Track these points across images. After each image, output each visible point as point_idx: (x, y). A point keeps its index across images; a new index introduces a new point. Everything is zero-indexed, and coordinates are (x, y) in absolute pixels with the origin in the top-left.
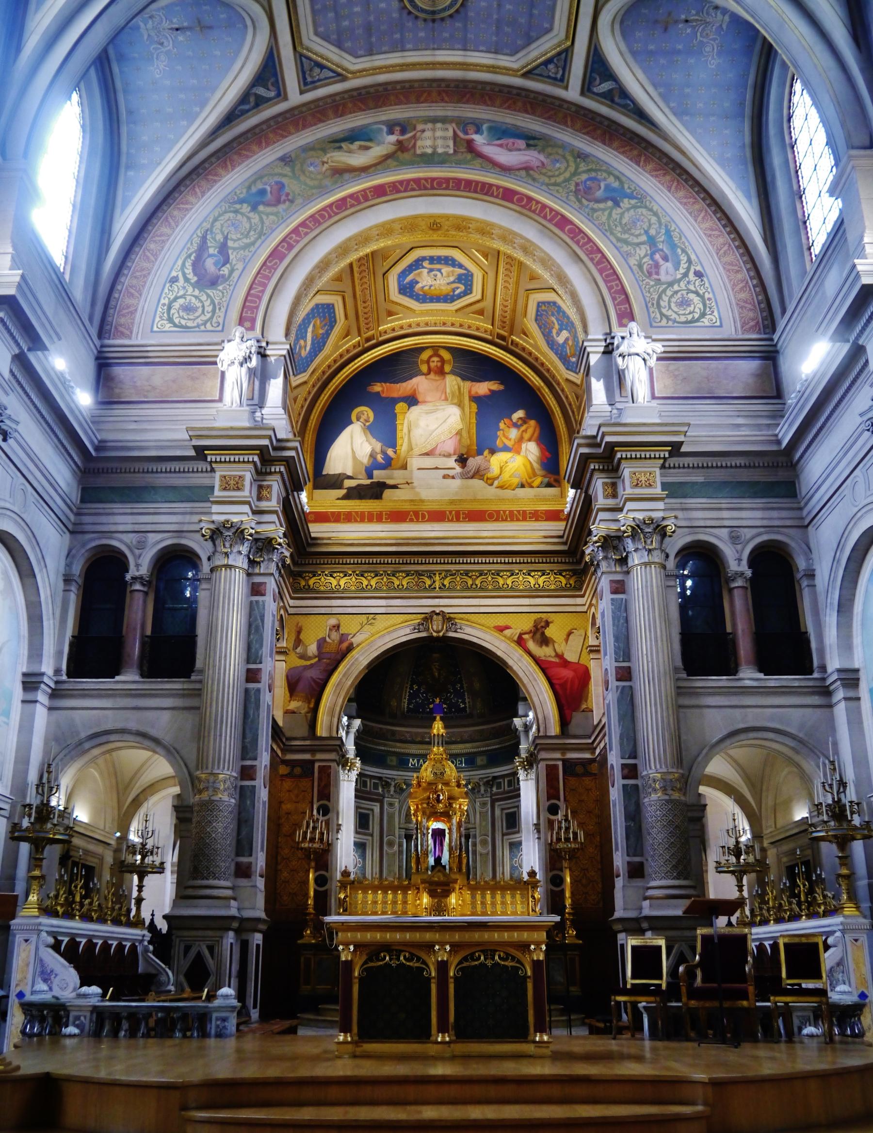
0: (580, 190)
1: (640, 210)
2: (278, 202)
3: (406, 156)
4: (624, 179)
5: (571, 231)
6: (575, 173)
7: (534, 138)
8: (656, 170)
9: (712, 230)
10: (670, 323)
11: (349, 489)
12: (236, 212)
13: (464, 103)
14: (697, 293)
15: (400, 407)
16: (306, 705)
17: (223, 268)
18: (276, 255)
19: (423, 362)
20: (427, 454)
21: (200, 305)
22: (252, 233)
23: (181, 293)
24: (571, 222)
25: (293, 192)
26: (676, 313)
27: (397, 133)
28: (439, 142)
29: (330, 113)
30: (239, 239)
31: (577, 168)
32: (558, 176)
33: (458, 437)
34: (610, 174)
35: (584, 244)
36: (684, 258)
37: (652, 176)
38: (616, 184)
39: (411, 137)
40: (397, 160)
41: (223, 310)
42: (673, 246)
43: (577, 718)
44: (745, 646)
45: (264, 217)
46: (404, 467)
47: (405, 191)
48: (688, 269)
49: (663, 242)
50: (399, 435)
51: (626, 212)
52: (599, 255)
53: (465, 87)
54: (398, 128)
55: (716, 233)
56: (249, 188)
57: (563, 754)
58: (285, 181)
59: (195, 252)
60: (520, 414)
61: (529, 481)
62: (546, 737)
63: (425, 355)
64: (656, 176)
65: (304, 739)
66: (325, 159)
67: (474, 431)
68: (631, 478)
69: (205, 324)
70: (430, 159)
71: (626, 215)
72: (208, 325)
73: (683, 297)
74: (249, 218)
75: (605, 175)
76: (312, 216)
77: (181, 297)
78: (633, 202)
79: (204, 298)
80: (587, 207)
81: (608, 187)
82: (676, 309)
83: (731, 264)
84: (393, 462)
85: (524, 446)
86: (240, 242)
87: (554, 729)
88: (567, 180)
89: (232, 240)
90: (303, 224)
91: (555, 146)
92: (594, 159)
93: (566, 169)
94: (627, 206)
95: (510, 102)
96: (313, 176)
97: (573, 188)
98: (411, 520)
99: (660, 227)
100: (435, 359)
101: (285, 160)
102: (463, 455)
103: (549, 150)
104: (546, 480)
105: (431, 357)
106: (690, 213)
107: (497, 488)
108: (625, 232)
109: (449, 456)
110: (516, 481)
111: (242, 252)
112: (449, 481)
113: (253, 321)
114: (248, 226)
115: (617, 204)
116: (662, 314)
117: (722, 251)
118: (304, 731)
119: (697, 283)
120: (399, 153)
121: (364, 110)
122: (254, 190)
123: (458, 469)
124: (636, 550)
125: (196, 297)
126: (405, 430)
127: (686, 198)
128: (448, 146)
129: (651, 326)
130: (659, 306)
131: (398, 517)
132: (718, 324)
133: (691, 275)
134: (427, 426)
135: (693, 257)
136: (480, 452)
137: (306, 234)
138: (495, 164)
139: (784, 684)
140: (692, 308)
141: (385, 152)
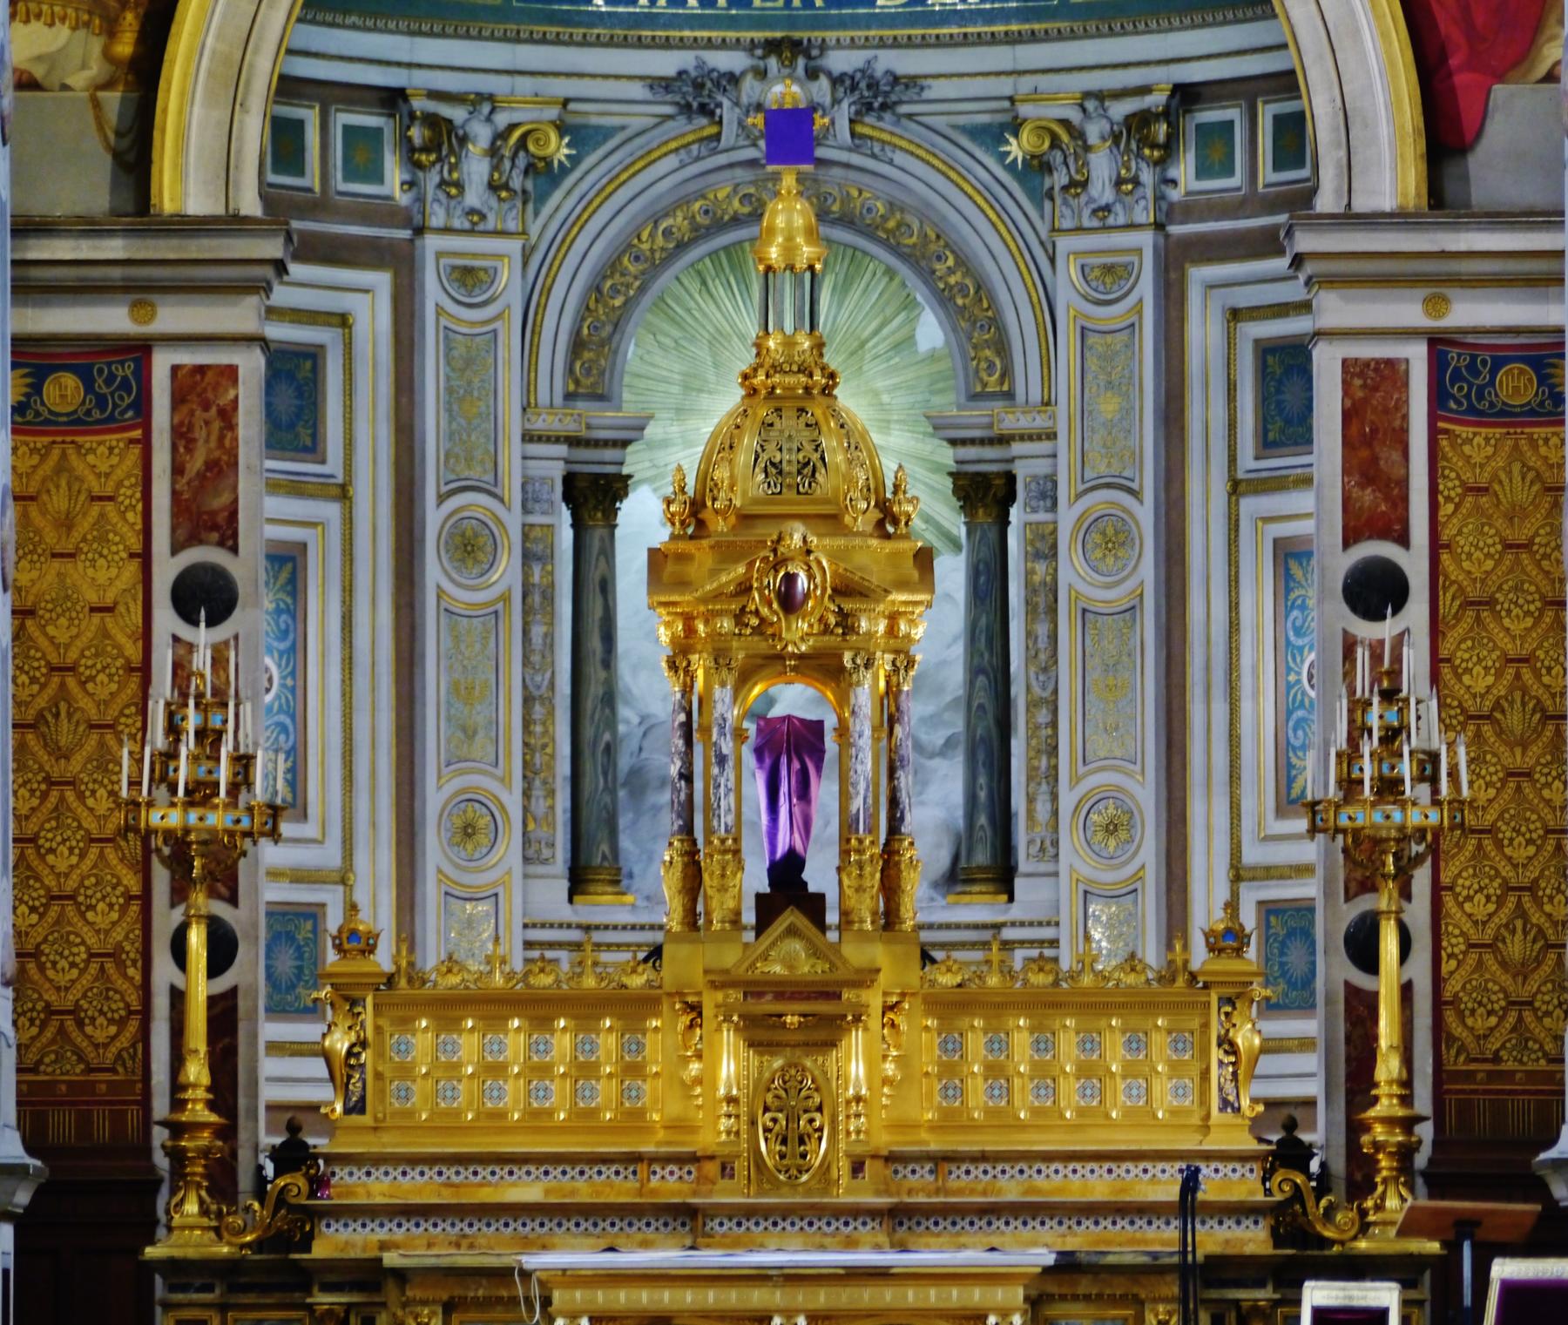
16: (96, 45)
43: (1510, 115)
57: (1436, 304)
62: (1350, 219)
65: (89, 227)
87: (1390, 171)
118: (88, 186)
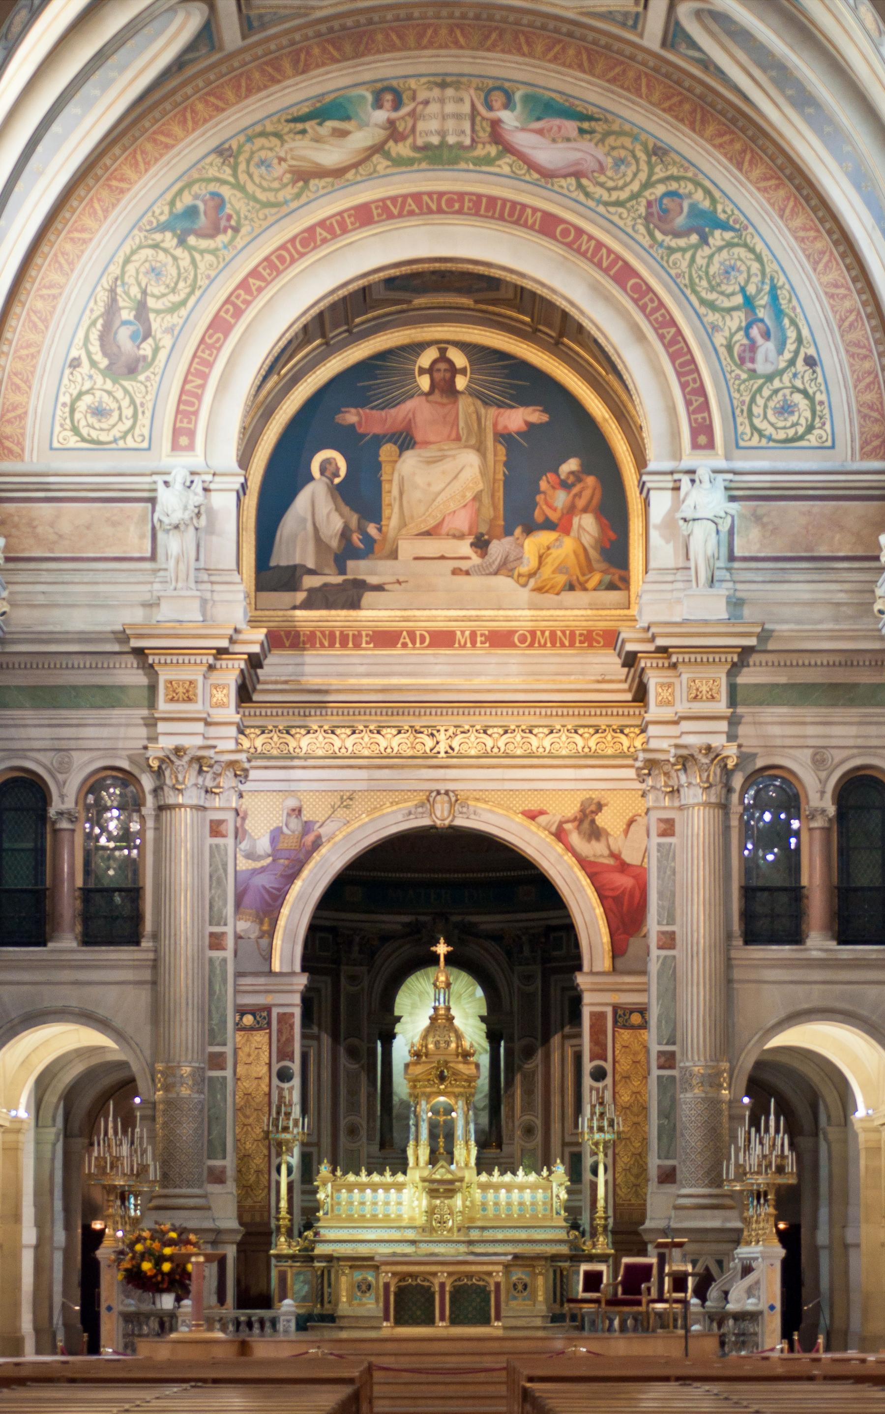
0: (652, 214)
1: (736, 250)
2: (215, 231)
3: (402, 149)
4: (717, 194)
5: (636, 288)
6: (646, 186)
7: (590, 118)
8: (766, 179)
9: (836, 286)
10: (764, 442)
11: (311, 591)
12: (156, 246)
13: (488, 50)
14: (805, 393)
15: (387, 451)
17: (144, 345)
18: (219, 326)
19: (422, 371)
20: (428, 534)
21: (114, 406)
22: (181, 285)
23: (87, 385)
24: (637, 275)
25: (238, 213)
26: (772, 425)
27: (388, 105)
28: (450, 124)
29: (287, 65)
30: (164, 295)
31: (651, 174)
32: (622, 188)
33: (477, 505)
34: (697, 184)
35: (655, 310)
36: (792, 334)
37: (758, 189)
38: (706, 204)
39: (409, 114)
40: (387, 155)
41: (148, 414)
42: (779, 313)
45: (198, 257)
46: (393, 555)
47: (400, 215)
48: (796, 353)
49: (764, 307)
50: (386, 499)
52: (673, 330)
53: (491, 18)
54: (389, 97)
55: (842, 291)
56: (172, 203)
58: (226, 192)
59: (102, 315)
60: (571, 465)
61: (582, 579)
63: (427, 358)
64: (765, 190)
66: (282, 154)
67: (500, 494)
68: (689, 688)
69: (124, 438)
70: (437, 155)
71: (716, 259)
72: (129, 438)
73: (785, 400)
74: (175, 258)
75: (690, 187)
76: (267, 259)
77: (87, 392)
78: (728, 235)
79: (120, 394)
80: (661, 245)
81: (693, 207)
82: (772, 419)
83: (857, 345)
84: (377, 547)
85: (576, 520)
86: (164, 300)
88: (634, 196)
89: (153, 296)
90: (254, 273)
91: (621, 133)
92: (677, 158)
93: (635, 175)
94: (720, 243)
95: (557, 48)
96: (265, 184)
97: (642, 210)
98: (405, 645)
99: (763, 283)
100: (442, 366)
101: (223, 152)
102: (482, 535)
103: (611, 140)
104: (608, 578)
105: (434, 362)
106: (808, 257)
107: (533, 590)
108: (712, 289)
109: (461, 537)
110: (561, 579)
111: (168, 317)
112: (461, 579)
113: (191, 434)
114: (174, 272)
115: (704, 240)
116: (754, 428)
117: (846, 324)
119: (806, 378)
120: (391, 143)
121: (338, 61)
122: (179, 207)
123: (476, 560)
124: (690, 784)
125: (109, 393)
126: (395, 492)
127: (804, 229)
128: (463, 132)
129: (738, 447)
130: (750, 411)
131: (386, 639)
132: (829, 443)
133: (800, 362)
134: (429, 485)
135: (805, 332)
136: (508, 532)
137: (260, 290)
138: (532, 166)
139: (859, 955)
140: (794, 418)
141: (369, 143)
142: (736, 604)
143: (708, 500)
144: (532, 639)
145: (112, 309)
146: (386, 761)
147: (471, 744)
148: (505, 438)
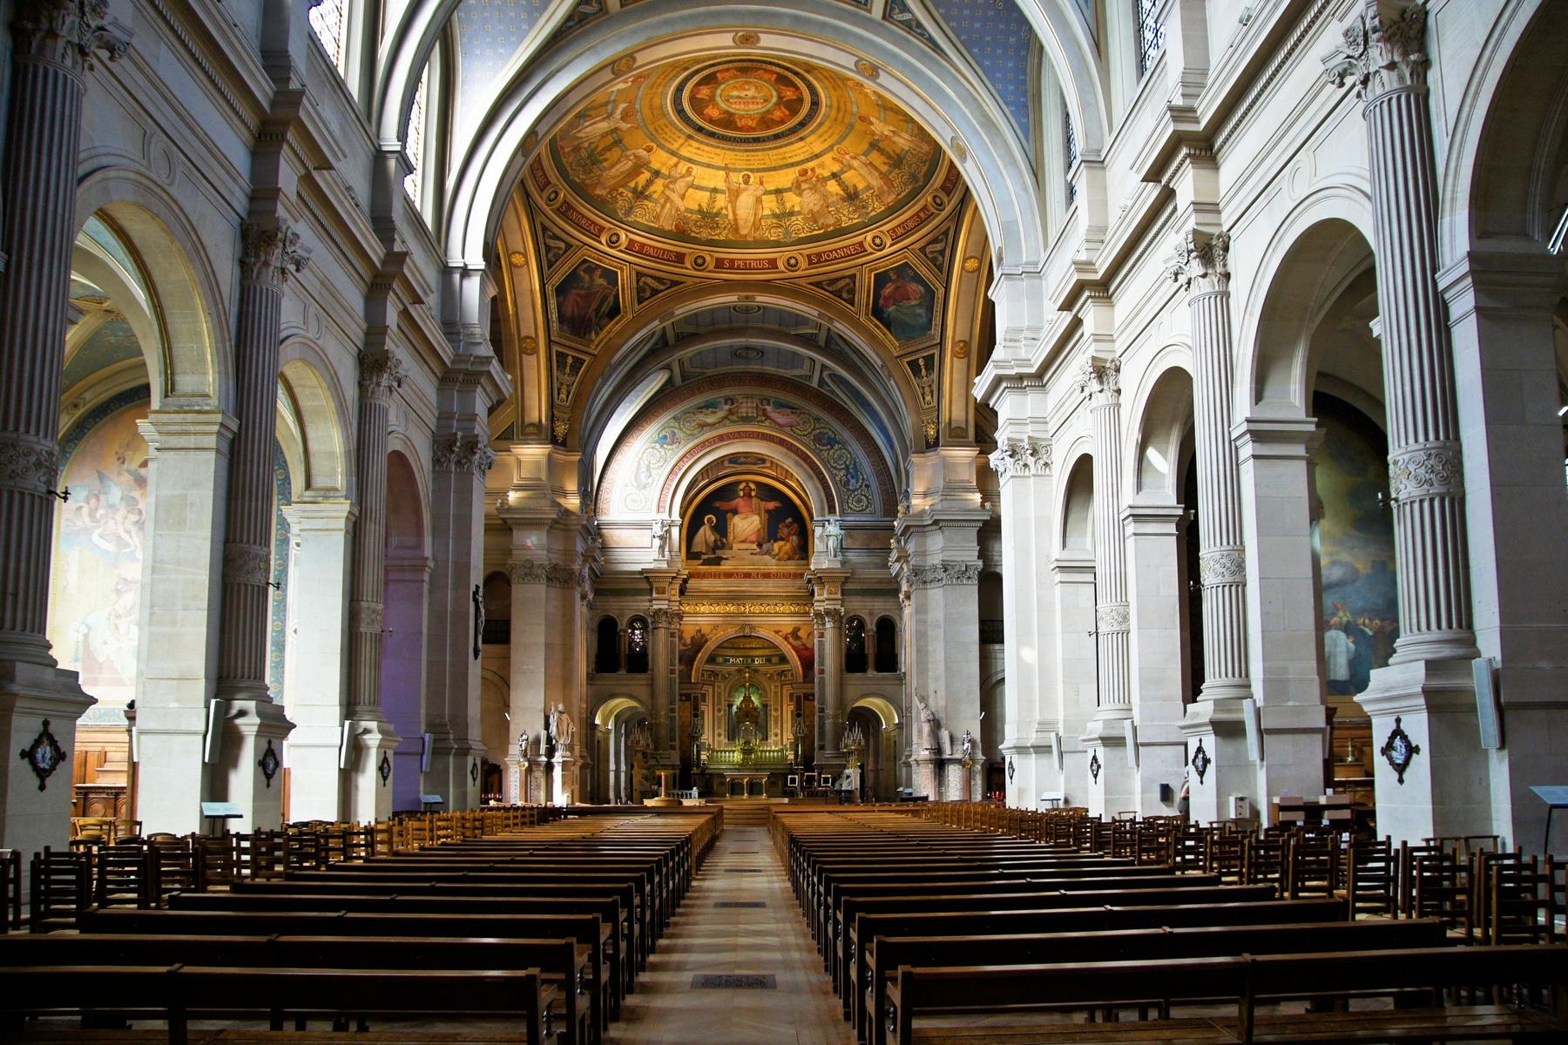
44: (871, 660)
51: (835, 452)
70: (746, 420)
131: (728, 575)
142: (843, 563)
143: (833, 529)
144: (776, 576)
145: (639, 467)
146: (728, 615)
147: (757, 609)
148: (767, 511)
